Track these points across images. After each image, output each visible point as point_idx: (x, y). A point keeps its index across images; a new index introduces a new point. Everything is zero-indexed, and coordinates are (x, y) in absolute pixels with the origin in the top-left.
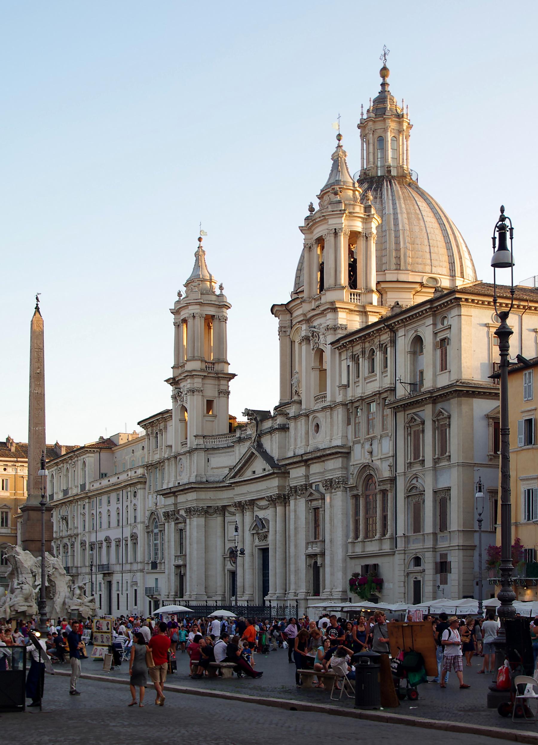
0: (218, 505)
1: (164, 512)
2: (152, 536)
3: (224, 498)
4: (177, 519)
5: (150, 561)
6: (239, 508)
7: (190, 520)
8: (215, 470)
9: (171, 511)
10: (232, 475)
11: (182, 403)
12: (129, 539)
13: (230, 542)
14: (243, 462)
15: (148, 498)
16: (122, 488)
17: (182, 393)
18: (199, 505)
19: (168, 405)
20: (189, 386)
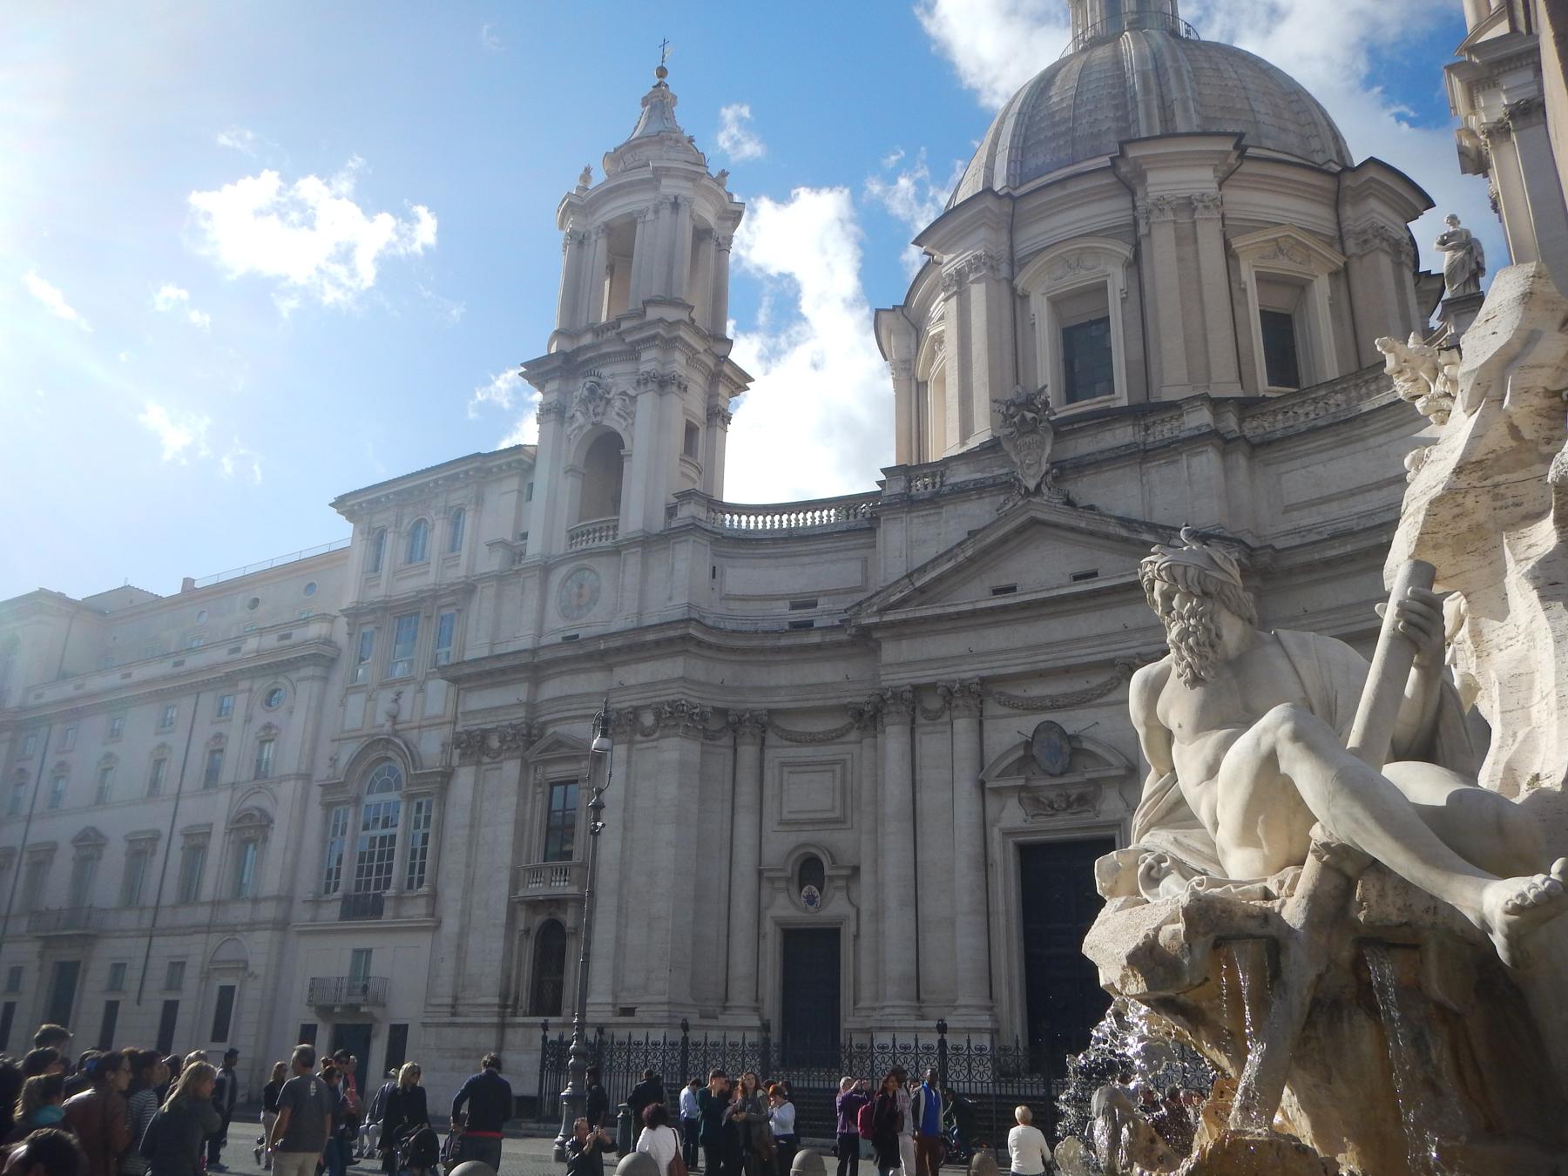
0: (749, 706)
1: (469, 733)
2: (356, 815)
3: (778, 687)
4: (559, 743)
5: (339, 894)
6: (904, 708)
7: (629, 750)
8: (732, 604)
9: (512, 726)
10: (893, 599)
11: (598, 418)
12: (220, 828)
13: (787, 828)
14: (969, 553)
15: (343, 703)
16: (197, 689)
17: (608, 393)
18: (691, 699)
19: (528, 433)
20: (645, 368)
